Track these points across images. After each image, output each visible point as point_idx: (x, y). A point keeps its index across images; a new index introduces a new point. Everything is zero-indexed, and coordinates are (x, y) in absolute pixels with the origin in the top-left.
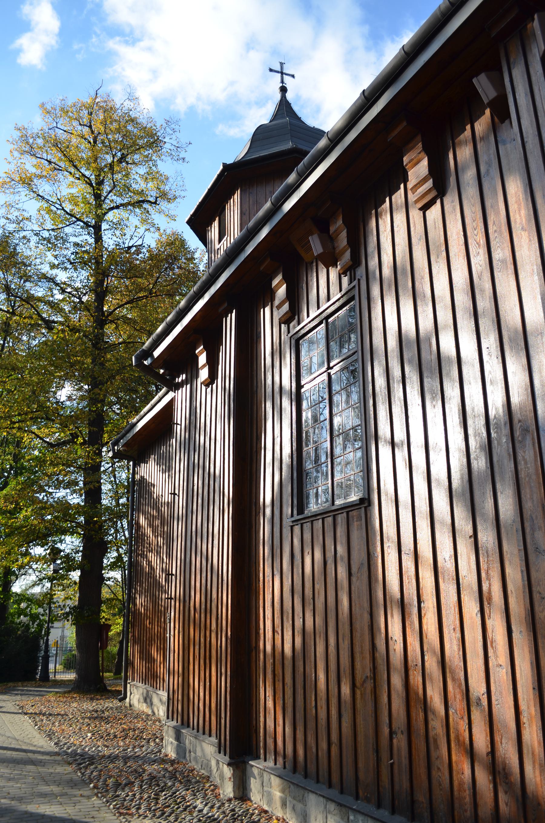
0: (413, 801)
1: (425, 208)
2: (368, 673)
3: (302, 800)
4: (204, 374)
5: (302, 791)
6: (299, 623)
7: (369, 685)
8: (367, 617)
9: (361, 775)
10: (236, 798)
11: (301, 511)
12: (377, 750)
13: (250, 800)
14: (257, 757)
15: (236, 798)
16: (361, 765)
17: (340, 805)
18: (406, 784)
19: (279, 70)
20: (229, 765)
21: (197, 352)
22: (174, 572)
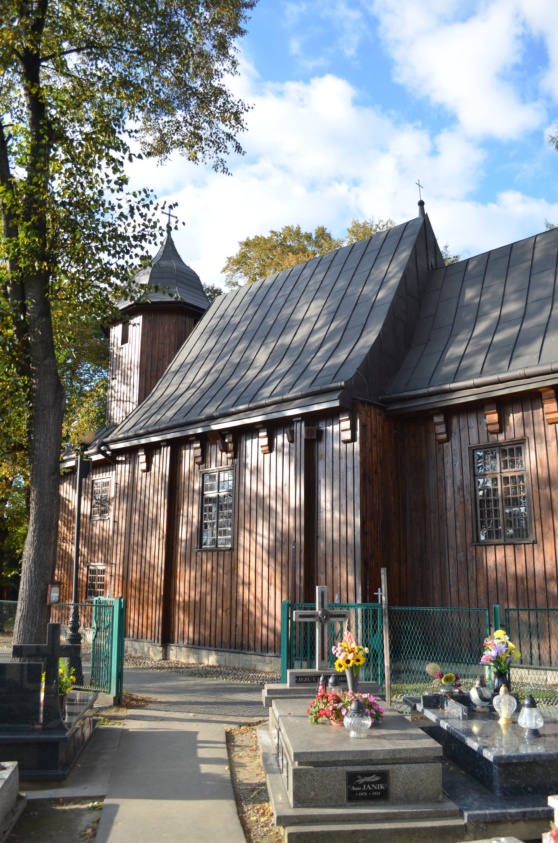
0: (242, 644)
1: (264, 454)
2: (229, 607)
3: (198, 654)
4: (144, 466)
5: (197, 650)
6: (198, 590)
7: (229, 611)
8: (229, 589)
9: (224, 640)
10: (163, 659)
11: (201, 547)
12: (230, 631)
13: (169, 659)
14: (173, 642)
15: (163, 659)
16: (224, 637)
17: (215, 650)
18: (240, 640)
19: (168, 213)
20: (161, 646)
21: (139, 454)
22: (114, 562)
